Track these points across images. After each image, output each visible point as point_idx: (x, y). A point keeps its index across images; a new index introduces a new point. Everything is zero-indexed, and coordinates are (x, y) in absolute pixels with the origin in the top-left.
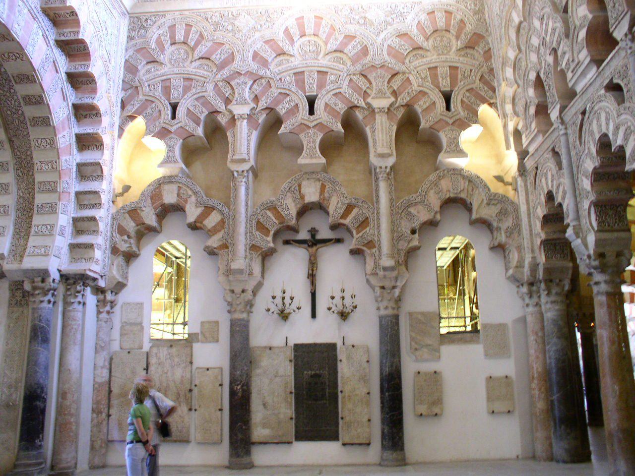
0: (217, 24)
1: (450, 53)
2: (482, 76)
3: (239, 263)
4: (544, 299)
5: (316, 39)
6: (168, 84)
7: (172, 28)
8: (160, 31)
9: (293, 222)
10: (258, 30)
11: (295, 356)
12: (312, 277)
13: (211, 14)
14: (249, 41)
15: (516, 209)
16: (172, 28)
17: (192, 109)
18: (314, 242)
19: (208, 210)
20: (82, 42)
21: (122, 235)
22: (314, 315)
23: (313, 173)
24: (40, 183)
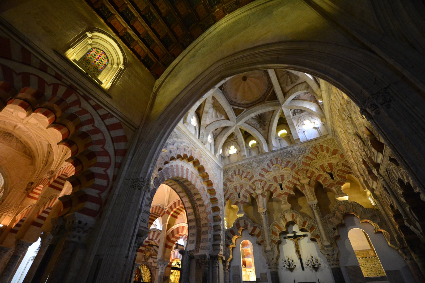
0: (247, 167)
1: (327, 158)
2: (343, 164)
5: (277, 165)
7: (235, 171)
8: (232, 172)
9: (285, 230)
10: (258, 166)
12: (298, 251)
13: (244, 165)
14: (257, 170)
16: (235, 171)
20: (210, 180)
21: (229, 240)
22: (303, 269)
23: (288, 210)
24: (203, 224)
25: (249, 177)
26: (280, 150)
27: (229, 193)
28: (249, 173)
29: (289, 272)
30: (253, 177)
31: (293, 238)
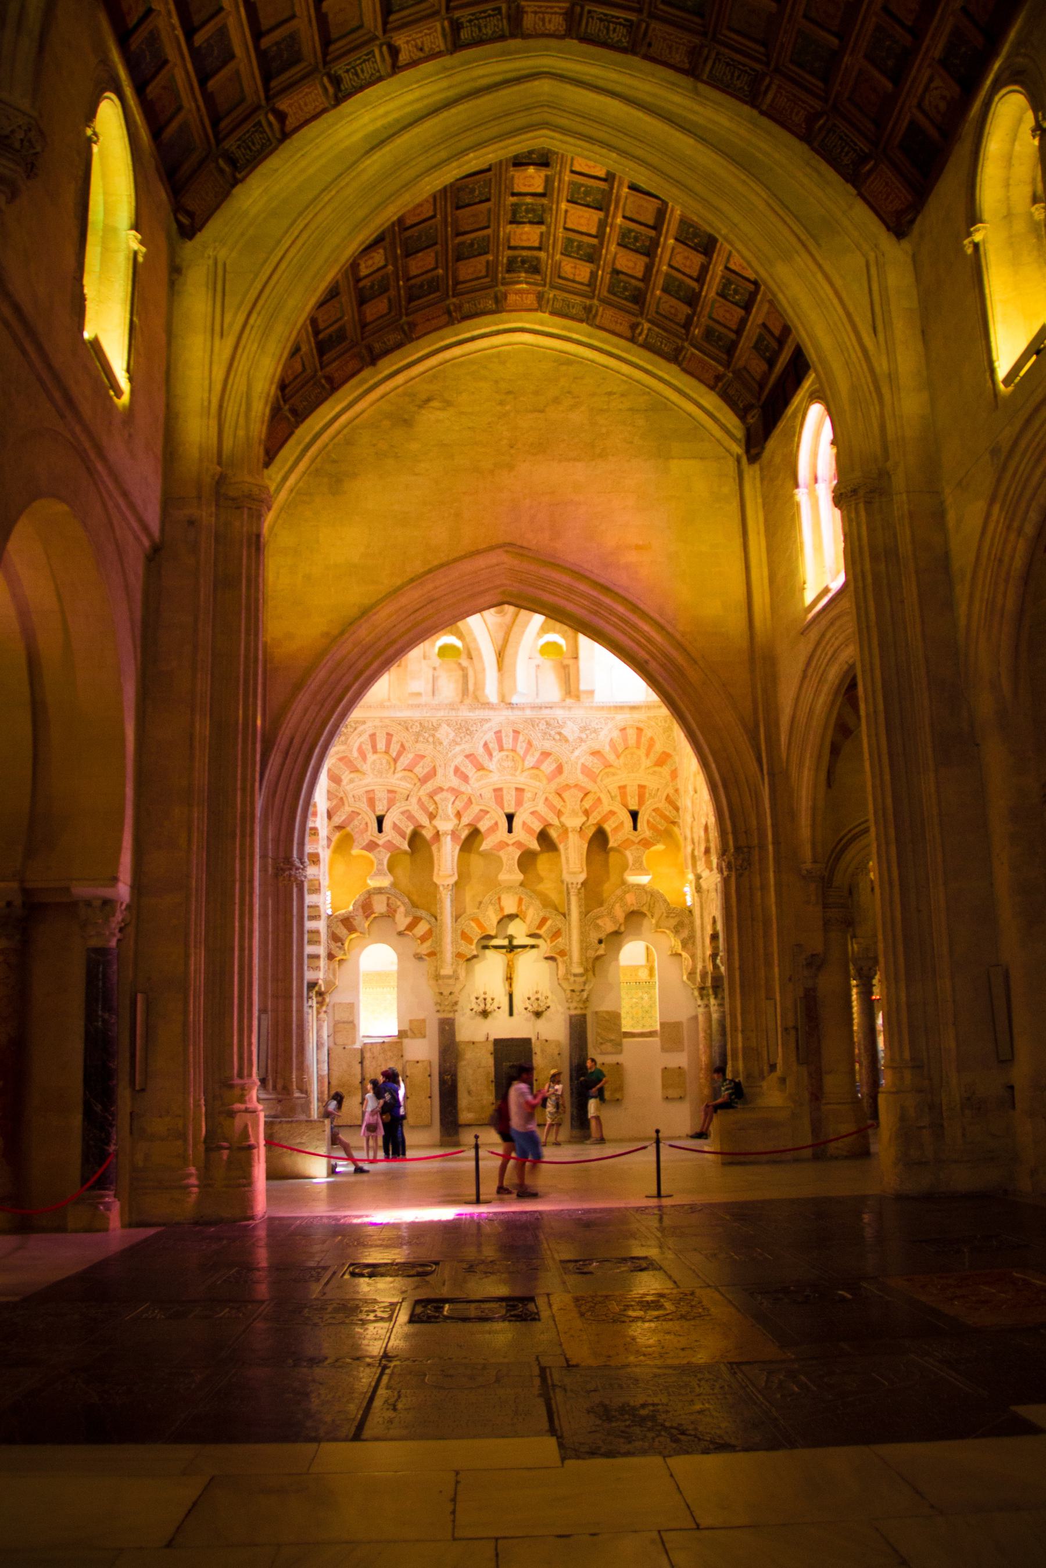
0: (418, 734)
2: (668, 796)
3: (447, 971)
4: (712, 1001)
6: (371, 795)
7: (373, 736)
8: (362, 739)
9: (493, 933)
10: (457, 744)
11: (495, 1050)
12: (509, 979)
15: (692, 923)
16: (373, 736)
17: (397, 822)
18: (511, 948)
19: (415, 922)
22: (511, 1014)
25: (420, 770)
26: (533, 708)
27: (347, 809)
28: (423, 757)
29: (480, 1020)
30: (433, 773)
31: (504, 951)
